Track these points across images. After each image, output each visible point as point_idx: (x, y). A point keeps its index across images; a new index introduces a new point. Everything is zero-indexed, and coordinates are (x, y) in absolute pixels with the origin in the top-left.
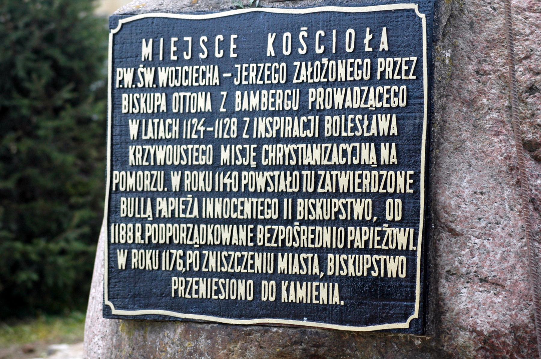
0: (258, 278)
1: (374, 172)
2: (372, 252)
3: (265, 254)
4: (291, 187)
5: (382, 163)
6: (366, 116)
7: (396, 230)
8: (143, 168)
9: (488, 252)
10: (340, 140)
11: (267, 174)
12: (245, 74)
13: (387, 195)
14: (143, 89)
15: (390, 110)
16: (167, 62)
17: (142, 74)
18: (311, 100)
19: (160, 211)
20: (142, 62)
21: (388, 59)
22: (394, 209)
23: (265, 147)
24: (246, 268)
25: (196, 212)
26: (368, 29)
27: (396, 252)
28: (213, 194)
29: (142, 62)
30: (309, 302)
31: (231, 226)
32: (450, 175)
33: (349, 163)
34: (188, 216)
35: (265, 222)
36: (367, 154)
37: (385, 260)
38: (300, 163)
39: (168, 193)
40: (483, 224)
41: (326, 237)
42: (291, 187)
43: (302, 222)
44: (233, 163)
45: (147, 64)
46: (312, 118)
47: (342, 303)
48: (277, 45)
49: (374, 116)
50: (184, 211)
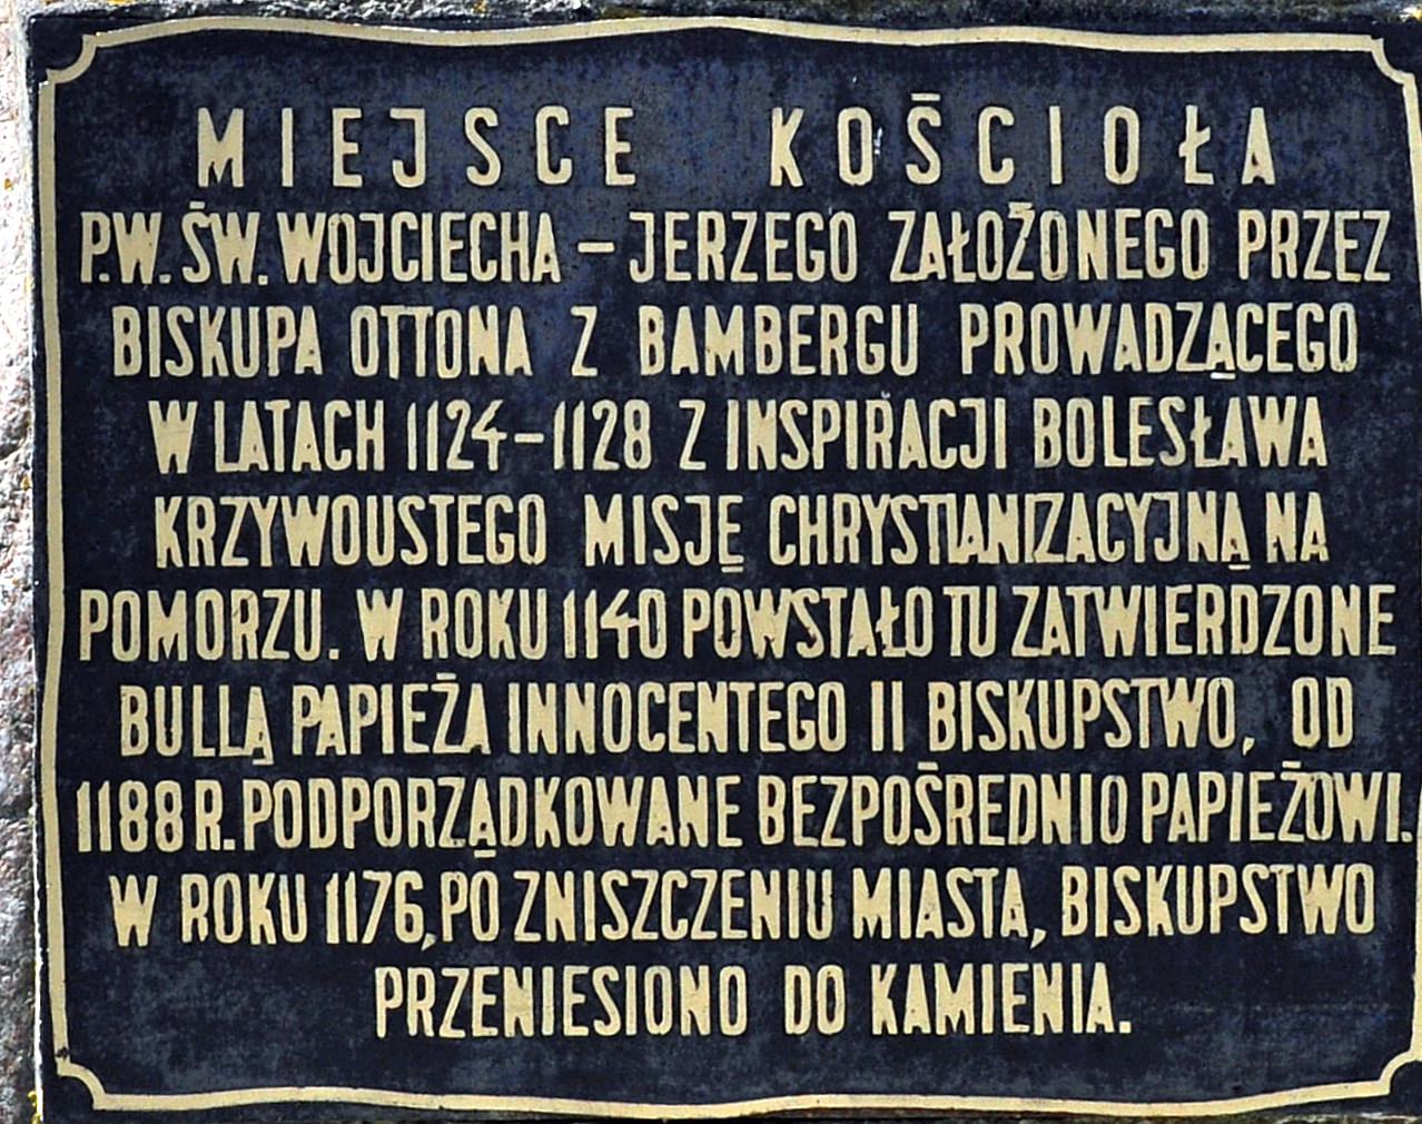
0: (768, 960)
1: (1238, 591)
2: (1246, 853)
3: (793, 875)
4: (899, 640)
5: (1272, 556)
6: (1199, 402)
8: (224, 580)
10: (1097, 480)
12: (673, 245)
14: (216, 293)
15: (1299, 384)
16: (315, 195)
17: (204, 235)
18: (968, 343)
19: (311, 734)
20: (200, 194)
21: (1277, 215)
22: (1326, 712)
23: (780, 502)
24: (712, 922)
25: (477, 734)
26: (1192, 112)
27: (1334, 852)
28: (556, 670)
29: (200, 194)
30: (987, 1028)
31: (639, 782)
33: (1140, 558)
34: (440, 746)
35: (788, 765)
36: (1210, 529)
37: (1293, 877)
38: (934, 559)
39: (347, 666)
41: (1052, 808)
42: (899, 640)
43: (952, 762)
44: (640, 559)
45: (221, 197)
46: (979, 404)
47: (1125, 1027)
48: (813, 145)
49: (1235, 403)
50: (424, 733)
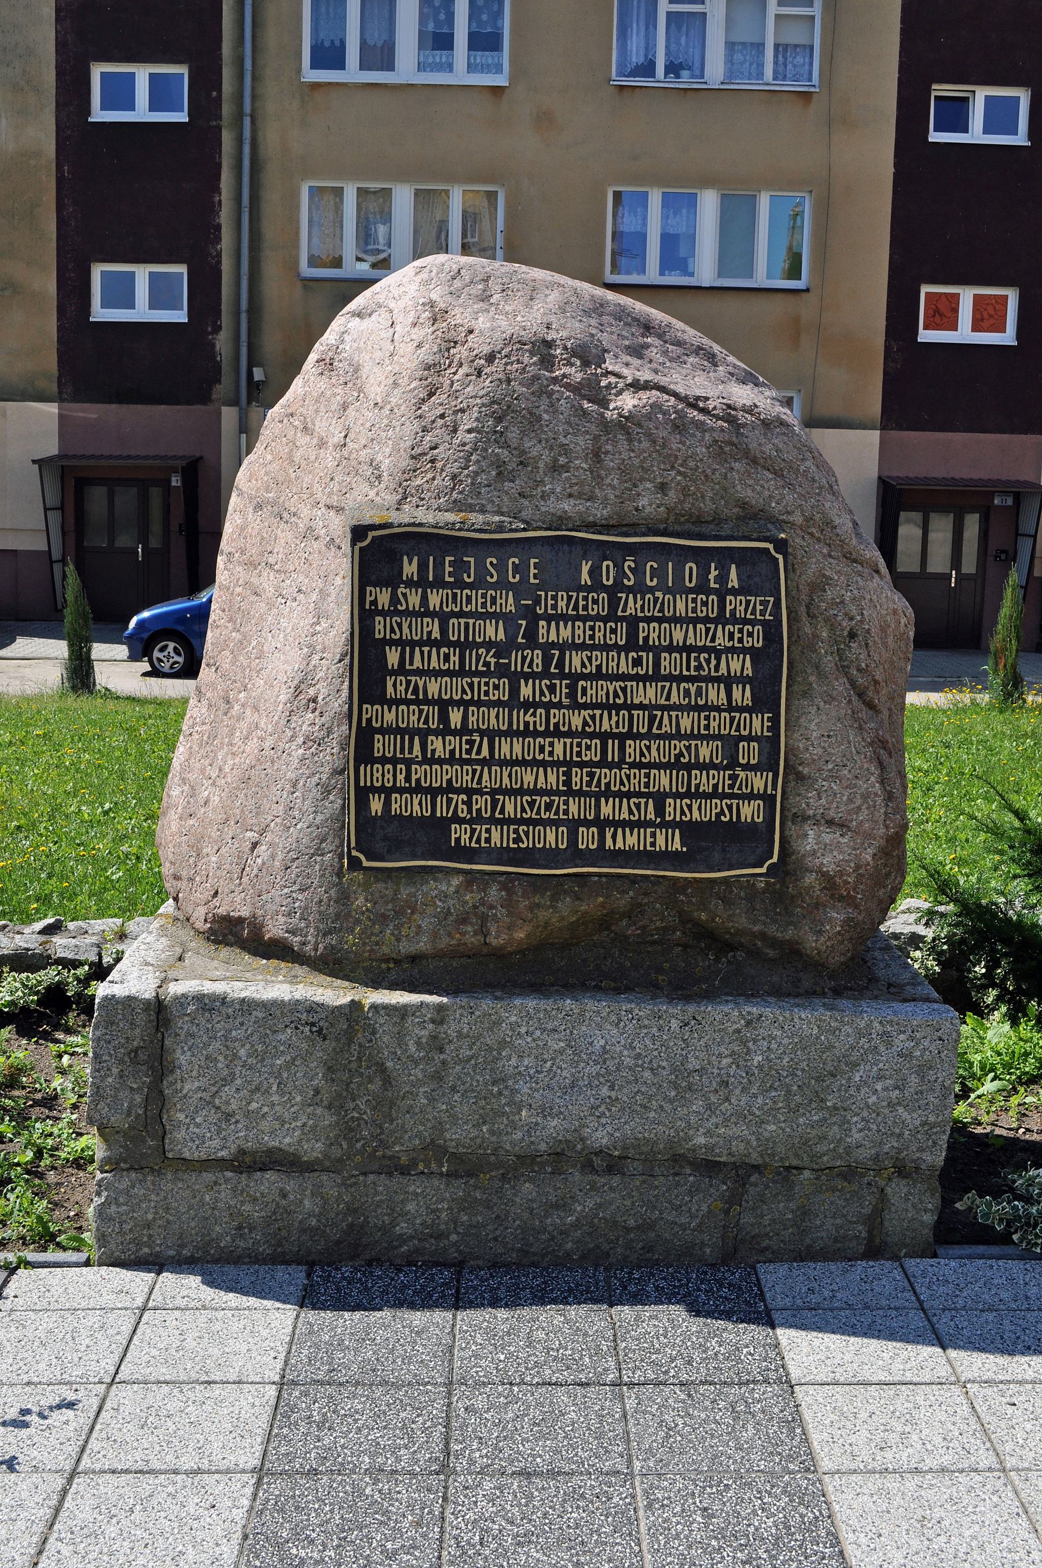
0: (573, 826)
1: (723, 714)
2: (724, 796)
3: (582, 799)
4: (617, 727)
5: (734, 704)
6: (713, 655)
7: (751, 774)
8: (408, 702)
9: (835, 794)
10: (680, 679)
11: (585, 713)
12: (550, 602)
13: (742, 738)
14: (408, 613)
15: (744, 651)
16: (439, 583)
17: (404, 595)
18: (641, 635)
19: (433, 751)
20: (403, 582)
21: (739, 598)
22: (750, 753)
23: (581, 683)
24: (557, 813)
25: (485, 752)
26: (713, 565)
27: (751, 797)
28: (510, 733)
29: (403, 582)
30: (642, 848)
31: (535, 769)
32: (799, 718)
33: (693, 703)
34: (474, 756)
35: (582, 765)
36: (715, 695)
37: (738, 804)
38: (629, 702)
39: (446, 730)
40: (830, 766)
41: (664, 780)
42: (617, 727)
43: (633, 765)
44: (537, 699)
45: (410, 583)
46: (644, 654)
47: (685, 849)
48: (595, 572)
49: (724, 656)
50: (469, 752)
